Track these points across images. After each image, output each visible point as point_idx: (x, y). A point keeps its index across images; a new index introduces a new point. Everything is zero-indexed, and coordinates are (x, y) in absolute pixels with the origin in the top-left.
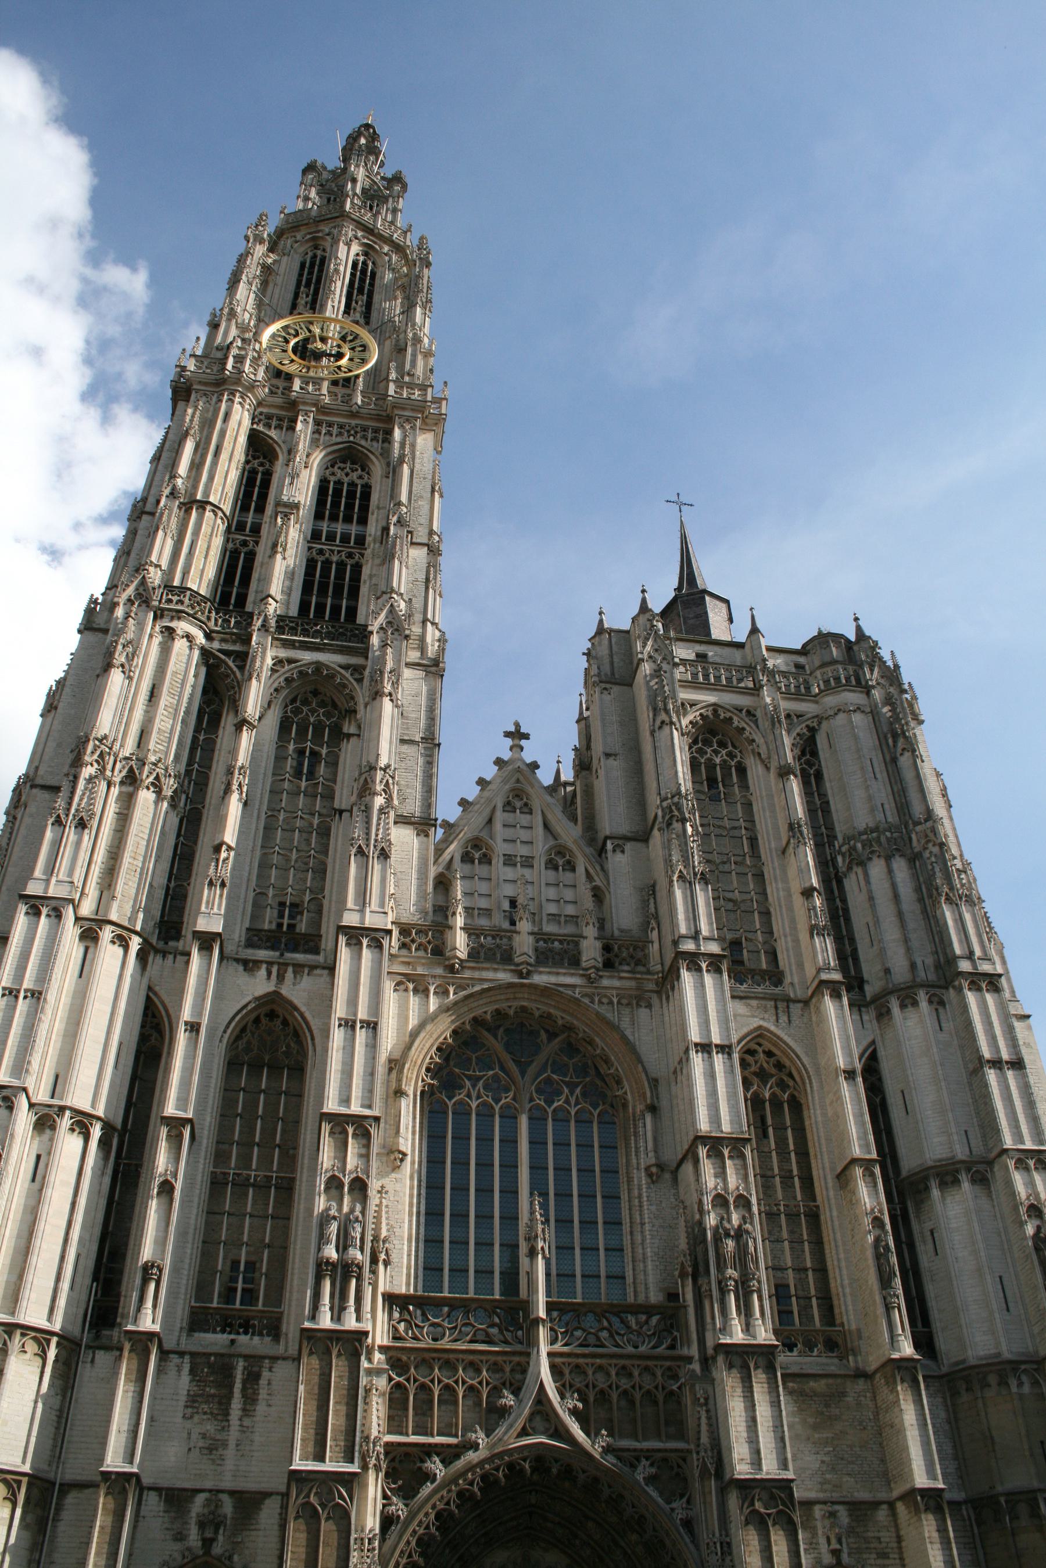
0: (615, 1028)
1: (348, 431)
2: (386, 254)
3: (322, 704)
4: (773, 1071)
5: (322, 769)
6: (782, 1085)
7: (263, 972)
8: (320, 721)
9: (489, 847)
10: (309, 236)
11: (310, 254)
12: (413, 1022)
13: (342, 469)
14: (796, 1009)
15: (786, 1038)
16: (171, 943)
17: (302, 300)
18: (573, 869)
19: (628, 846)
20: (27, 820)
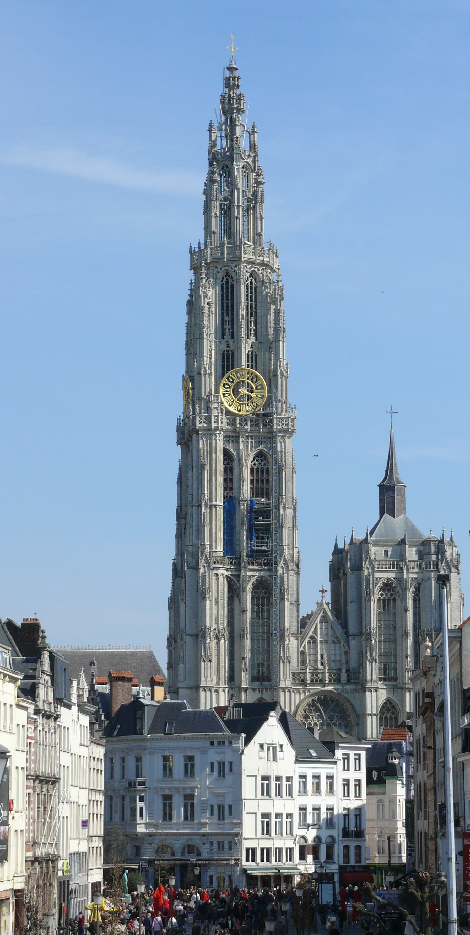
0: (348, 701)
1: (259, 442)
2: (261, 273)
3: (263, 589)
4: (391, 708)
5: (265, 615)
6: (393, 713)
7: (258, 691)
8: (263, 596)
9: (315, 639)
10: (224, 269)
11: (225, 280)
12: (297, 702)
13: (257, 460)
14: (399, 690)
15: (396, 701)
16: (232, 683)
17: (228, 327)
18: (340, 643)
19: (356, 638)
20: (187, 648)
